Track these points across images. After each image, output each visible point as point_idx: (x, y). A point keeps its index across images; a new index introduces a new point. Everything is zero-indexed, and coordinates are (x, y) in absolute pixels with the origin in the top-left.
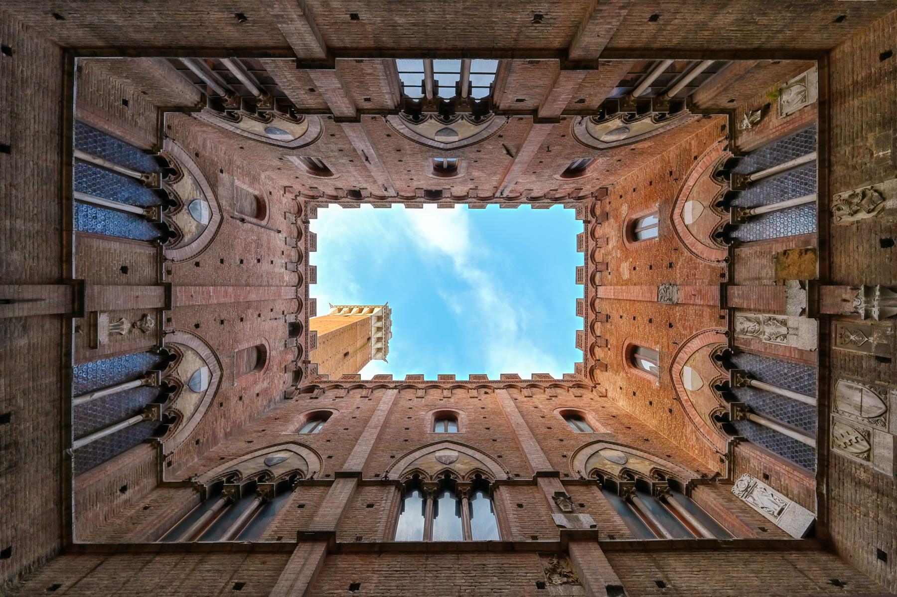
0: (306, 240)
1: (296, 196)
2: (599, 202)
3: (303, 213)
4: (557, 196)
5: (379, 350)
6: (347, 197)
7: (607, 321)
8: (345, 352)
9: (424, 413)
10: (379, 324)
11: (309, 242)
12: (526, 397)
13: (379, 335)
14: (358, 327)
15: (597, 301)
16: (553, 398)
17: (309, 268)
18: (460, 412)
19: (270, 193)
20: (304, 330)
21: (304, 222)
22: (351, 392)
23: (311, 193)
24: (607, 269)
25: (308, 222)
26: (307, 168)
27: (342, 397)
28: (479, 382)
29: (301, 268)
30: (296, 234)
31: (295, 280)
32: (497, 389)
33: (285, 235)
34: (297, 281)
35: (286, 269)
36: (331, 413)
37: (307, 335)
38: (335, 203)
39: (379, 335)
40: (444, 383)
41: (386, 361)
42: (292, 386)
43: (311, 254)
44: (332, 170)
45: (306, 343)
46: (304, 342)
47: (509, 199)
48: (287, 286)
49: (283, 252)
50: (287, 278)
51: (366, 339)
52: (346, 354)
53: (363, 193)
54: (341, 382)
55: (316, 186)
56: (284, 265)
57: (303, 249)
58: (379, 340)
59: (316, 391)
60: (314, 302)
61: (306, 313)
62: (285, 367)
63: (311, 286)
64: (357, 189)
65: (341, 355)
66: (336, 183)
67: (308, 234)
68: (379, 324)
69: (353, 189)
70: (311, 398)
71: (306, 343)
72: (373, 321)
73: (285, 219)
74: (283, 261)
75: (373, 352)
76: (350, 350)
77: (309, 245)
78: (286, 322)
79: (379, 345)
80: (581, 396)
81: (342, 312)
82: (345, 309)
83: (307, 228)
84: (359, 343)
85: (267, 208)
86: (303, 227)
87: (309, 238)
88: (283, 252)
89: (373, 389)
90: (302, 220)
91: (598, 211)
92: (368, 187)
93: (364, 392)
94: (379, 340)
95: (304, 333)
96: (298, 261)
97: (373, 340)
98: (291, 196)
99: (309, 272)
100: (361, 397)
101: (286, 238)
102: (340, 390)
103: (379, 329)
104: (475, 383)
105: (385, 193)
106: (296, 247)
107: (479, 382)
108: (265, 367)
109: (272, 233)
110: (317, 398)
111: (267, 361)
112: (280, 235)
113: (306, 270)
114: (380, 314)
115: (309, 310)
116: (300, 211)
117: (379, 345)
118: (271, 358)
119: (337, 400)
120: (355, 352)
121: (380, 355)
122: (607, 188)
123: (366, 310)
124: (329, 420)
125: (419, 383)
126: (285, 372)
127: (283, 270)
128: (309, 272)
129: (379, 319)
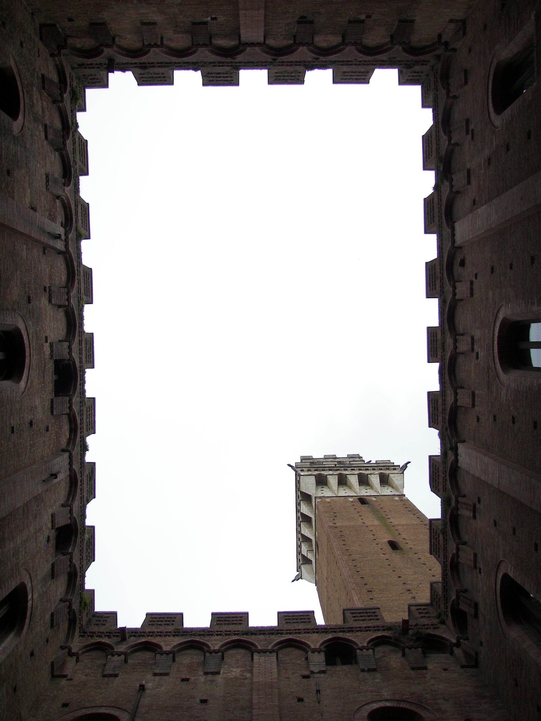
0: (160, 634)
1: (71, 654)
2: (70, 41)
4: (58, 124)
5: (384, 480)
6: (71, 554)
7: (311, 22)
8: (388, 548)
9: (504, 392)
10: (333, 481)
11: (162, 629)
12: (469, 183)
13: (353, 480)
14: (337, 525)
15: (271, 42)
16: (472, 127)
17: (217, 628)
18: (501, 316)
19: (65, 705)
20: (341, 635)
21: (124, 639)
22: (466, 538)
23: (64, 626)
24: (205, 23)
25: (123, 629)
26: (12, 635)
27: (475, 555)
28: (442, 279)
29: (216, 643)
30: (148, 655)
31: (239, 654)
32: (454, 242)
33: (149, 676)
34: (242, 651)
35: (218, 673)
36: (505, 576)
37: (351, 630)
38: (83, 576)
39: (353, 480)
40: (444, 350)
41: (405, 466)
42: (452, 653)
43: (188, 623)
44: (13, 585)
45: (367, 629)
46: (364, 634)
47: (68, 222)
48: (251, 672)
49: (183, 680)
50: (236, 672)
51: (364, 508)
52: (394, 545)
53: (62, 521)
54: (445, 557)
55: (48, 616)
56: (210, 677)
57: (177, 641)
58: (364, 481)
59: (463, 607)
60: (283, 616)
61: (307, 631)
62: (413, 669)
63: (253, 622)
64: (53, 534)
65: (396, 557)
66: (39, 577)
67: (148, 630)
68: (333, 481)
69: (53, 542)
70: (476, 616)
71: (367, 629)
72: (326, 492)
73: (116, 676)
74: (202, 679)
75: (387, 491)
77: (170, 628)
78: (324, 672)
79: (375, 480)
80: (466, 72)
81: (310, 556)
82: (304, 551)
83: (134, 632)
84: (372, 521)
85: (94, 711)
86: (133, 641)
87: (154, 629)
88: (183, 680)
89: (460, 494)
90: (118, 643)
91: (88, 43)
92: (50, 511)
93: (465, 513)
94: (364, 481)
95: (348, 636)
96: (201, 649)
97: (364, 492)
98: (71, 663)
99: (225, 628)
100: (474, 517)
101: (155, 674)
102: (462, 560)
103: (342, 481)
104: (442, 287)
105: (63, 476)
106: (173, 654)
107: (442, 279)
108: (413, 708)
109: (145, 701)
110: (476, 606)
111: (402, 705)
112: (149, 685)
113: (220, 634)
114: (313, 480)
115: (301, 626)
116: (100, 647)
117: (375, 480)
118: (397, 697)
119: (480, 565)
120: (389, 528)
121: (394, 478)
122: (42, 26)
123: (305, 509)
124: (518, 580)
125: (444, 401)
126: (425, 668)
127: (219, 679)
128: (225, 628)
129: (321, 481)
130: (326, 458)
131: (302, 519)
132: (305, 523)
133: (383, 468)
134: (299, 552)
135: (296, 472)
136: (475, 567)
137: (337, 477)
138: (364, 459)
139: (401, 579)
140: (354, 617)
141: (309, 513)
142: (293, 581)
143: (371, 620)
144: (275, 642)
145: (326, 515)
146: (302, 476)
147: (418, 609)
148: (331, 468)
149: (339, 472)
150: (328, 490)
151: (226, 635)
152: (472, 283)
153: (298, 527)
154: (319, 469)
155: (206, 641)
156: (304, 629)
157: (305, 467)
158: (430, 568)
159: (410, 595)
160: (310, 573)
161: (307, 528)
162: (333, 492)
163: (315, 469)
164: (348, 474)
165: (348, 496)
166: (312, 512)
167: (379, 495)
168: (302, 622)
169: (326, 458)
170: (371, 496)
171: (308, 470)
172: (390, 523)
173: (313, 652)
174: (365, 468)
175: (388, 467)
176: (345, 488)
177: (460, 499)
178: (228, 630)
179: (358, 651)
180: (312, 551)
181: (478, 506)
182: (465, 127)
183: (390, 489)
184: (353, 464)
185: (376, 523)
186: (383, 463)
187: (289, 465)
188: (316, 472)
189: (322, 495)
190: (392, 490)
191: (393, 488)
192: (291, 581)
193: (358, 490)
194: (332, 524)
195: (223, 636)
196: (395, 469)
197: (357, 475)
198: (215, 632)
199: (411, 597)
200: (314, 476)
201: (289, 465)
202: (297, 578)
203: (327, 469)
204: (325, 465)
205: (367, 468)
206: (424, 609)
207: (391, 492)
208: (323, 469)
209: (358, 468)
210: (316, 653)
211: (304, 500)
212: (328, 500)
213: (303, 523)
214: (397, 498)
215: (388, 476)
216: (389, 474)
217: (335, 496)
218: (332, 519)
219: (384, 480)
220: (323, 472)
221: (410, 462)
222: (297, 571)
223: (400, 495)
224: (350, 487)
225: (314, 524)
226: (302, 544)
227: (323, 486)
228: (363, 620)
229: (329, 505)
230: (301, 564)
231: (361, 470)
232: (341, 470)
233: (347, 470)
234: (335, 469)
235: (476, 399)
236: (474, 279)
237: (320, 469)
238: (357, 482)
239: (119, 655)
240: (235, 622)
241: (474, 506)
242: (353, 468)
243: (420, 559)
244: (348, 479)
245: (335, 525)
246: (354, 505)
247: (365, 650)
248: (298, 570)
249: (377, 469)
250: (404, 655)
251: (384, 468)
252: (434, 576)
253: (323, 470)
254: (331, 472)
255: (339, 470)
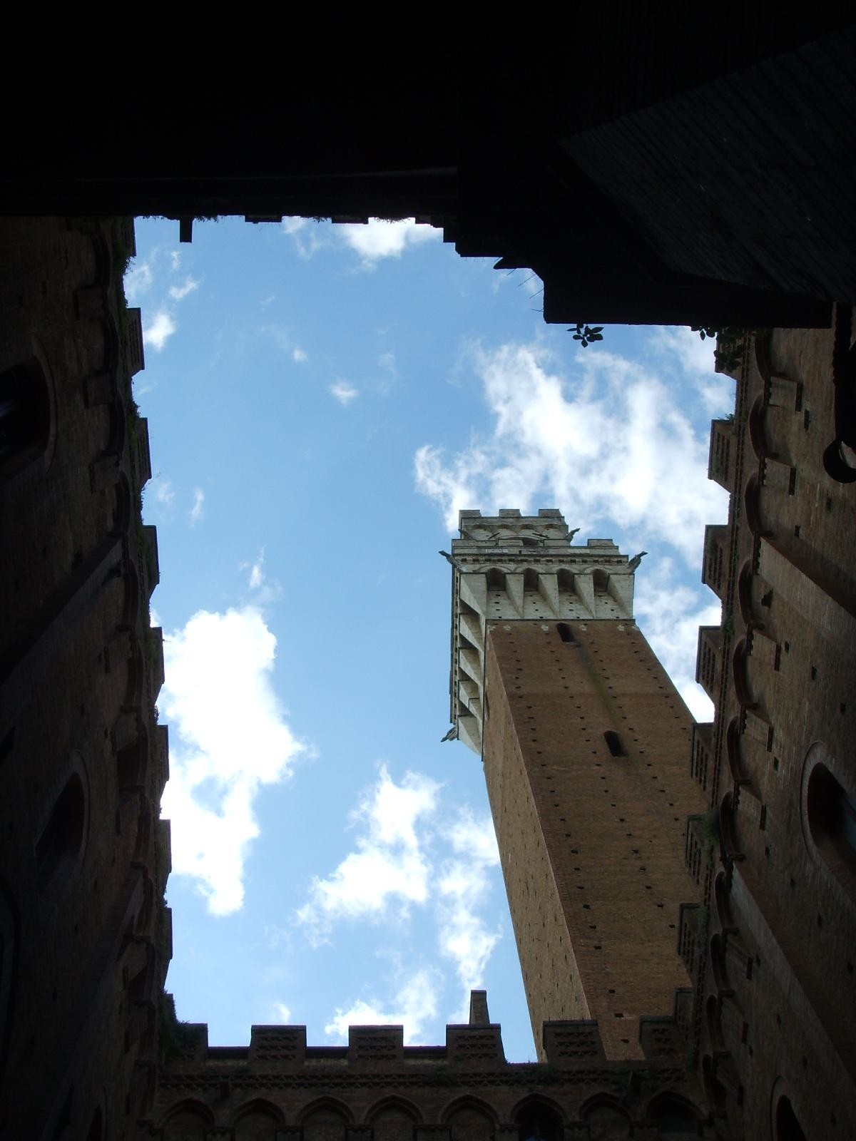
3: (198, 1096)
8: (603, 747)
10: (516, 585)
13: (550, 584)
16: (807, 406)
27: (746, 1026)
36: (784, 1102)
39: (550, 584)
41: (636, 561)
52: (614, 743)
57: (301, 1099)
58: (567, 584)
68: (516, 585)
76: (600, 725)
79: (586, 585)
81: (473, 709)
84: (581, 686)
94: (567, 584)
97: (568, 611)
100: (749, 977)
103: (532, 583)
114: (481, 582)
117: (586, 585)
121: (617, 582)
123: (466, 630)
129: (496, 583)
130: (503, 518)
131: (462, 644)
132: (467, 651)
133: (600, 559)
134: (454, 694)
135: (454, 566)
136: (744, 1041)
137: (522, 578)
138: (567, 521)
139: (624, 824)
140: (561, 1044)
141: (475, 640)
142: (444, 740)
143: (585, 1052)
144: (446, 1106)
145: (503, 665)
146: (464, 575)
147: (655, 1030)
148: (513, 558)
149: (525, 566)
150: (507, 602)
151: (376, 1084)
152: (778, 650)
153: (454, 653)
154: (492, 558)
155: (346, 1101)
156: (489, 1074)
157: (469, 555)
158: (671, 802)
159: (638, 863)
160: (473, 734)
161: (470, 662)
162: (516, 609)
163: (487, 557)
164: (541, 574)
165: (542, 619)
166: (479, 639)
167: (592, 618)
168: (486, 1055)
169: (503, 518)
170: (578, 620)
171: (476, 561)
172: (609, 690)
173: (502, 1131)
174: (569, 559)
175: (607, 559)
176: (536, 598)
177: (730, 937)
178: (376, 1071)
179: (566, 1130)
180: (477, 700)
181: (755, 965)
182: (795, 393)
183: (611, 604)
184: (550, 547)
185: (587, 688)
186: (600, 547)
187: (443, 553)
188: (488, 564)
189: (495, 615)
190: (615, 607)
191: (615, 601)
192: (441, 739)
193: (556, 607)
194: (514, 689)
195: (370, 1087)
196: (620, 562)
197: (556, 575)
198: (357, 1079)
199: (638, 869)
200: (484, 575)
201: (443, 553)
202: (452, 737)
203: (506, 558)
204: (502, 547)
205: (573, 559)
206: (664, 1031)
207: (612, 610)
208: (499, 558)
209: (557, 559)
210: (507, 1132)
211: (466, 614)
212: (507, 628)
213: (464, 650)
214: (621, 628)
215: (609, 577)
216: (609, 574)
217: (519, 618)
218: (514, 677)
219: (602, 584)
220: (500, 567)
221: (646, 553)
222: (451, 722)
223: (625, 620)
224: (545, 598)
225: (482, 664)
226: (461, 686)
227: (500, 593)
228: (575, 1053)
229: (509, 641)
230: (459, 716)
231: (562, 561)
232: (530, 561)
233: (539, 561)
234: (520, 558)
235: (767, 821)
236: (783, 647)
237: (496, 558)
238: (555, 589)
239: (223, 1134)
240: (385, 1052)
241: (750, 962)
242: (551, 558)
243: (656, 778)
244: (542, 583)
245: (519, 692)
246: (549, 643)
247: (576, 1130)
248: (453, 720)
249: (591, 561)
250: (631, 1135)
251: (602, 559)
252: (676, 819)
253: (499, 561)
254: (512, 566)
255: (526, 561)
